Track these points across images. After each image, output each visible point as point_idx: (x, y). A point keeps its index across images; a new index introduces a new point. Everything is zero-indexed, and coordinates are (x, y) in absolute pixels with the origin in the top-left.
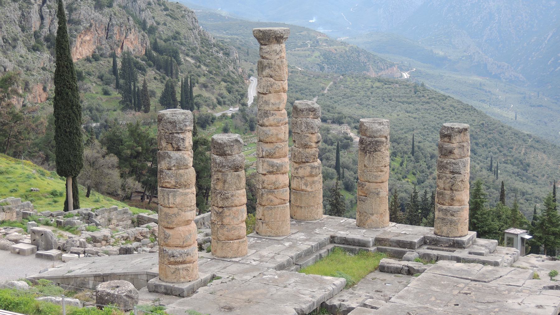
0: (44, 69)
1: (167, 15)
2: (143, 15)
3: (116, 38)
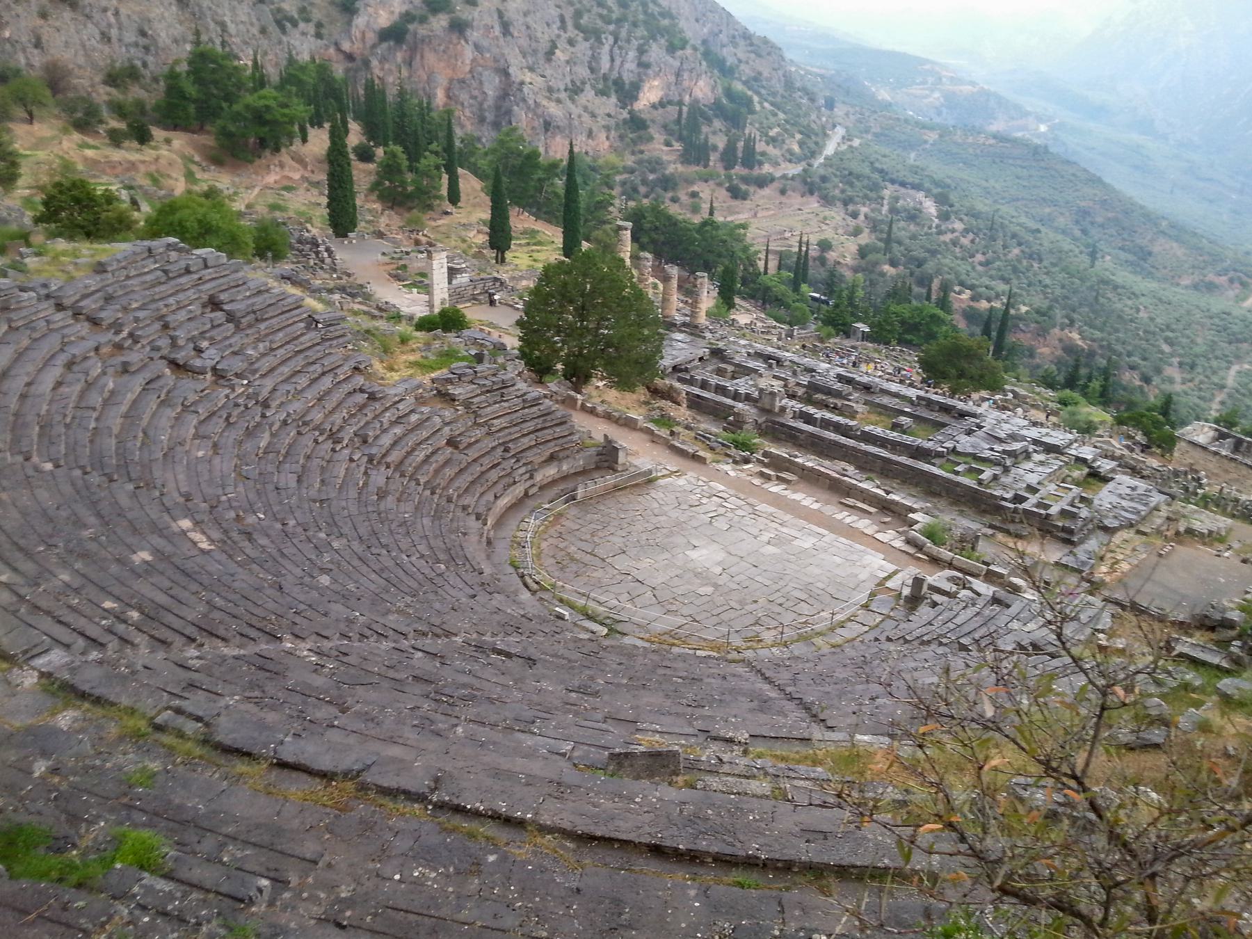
0: (609, 115)
1: (752, 52)
2: (725, 50)
3: (686, 84)
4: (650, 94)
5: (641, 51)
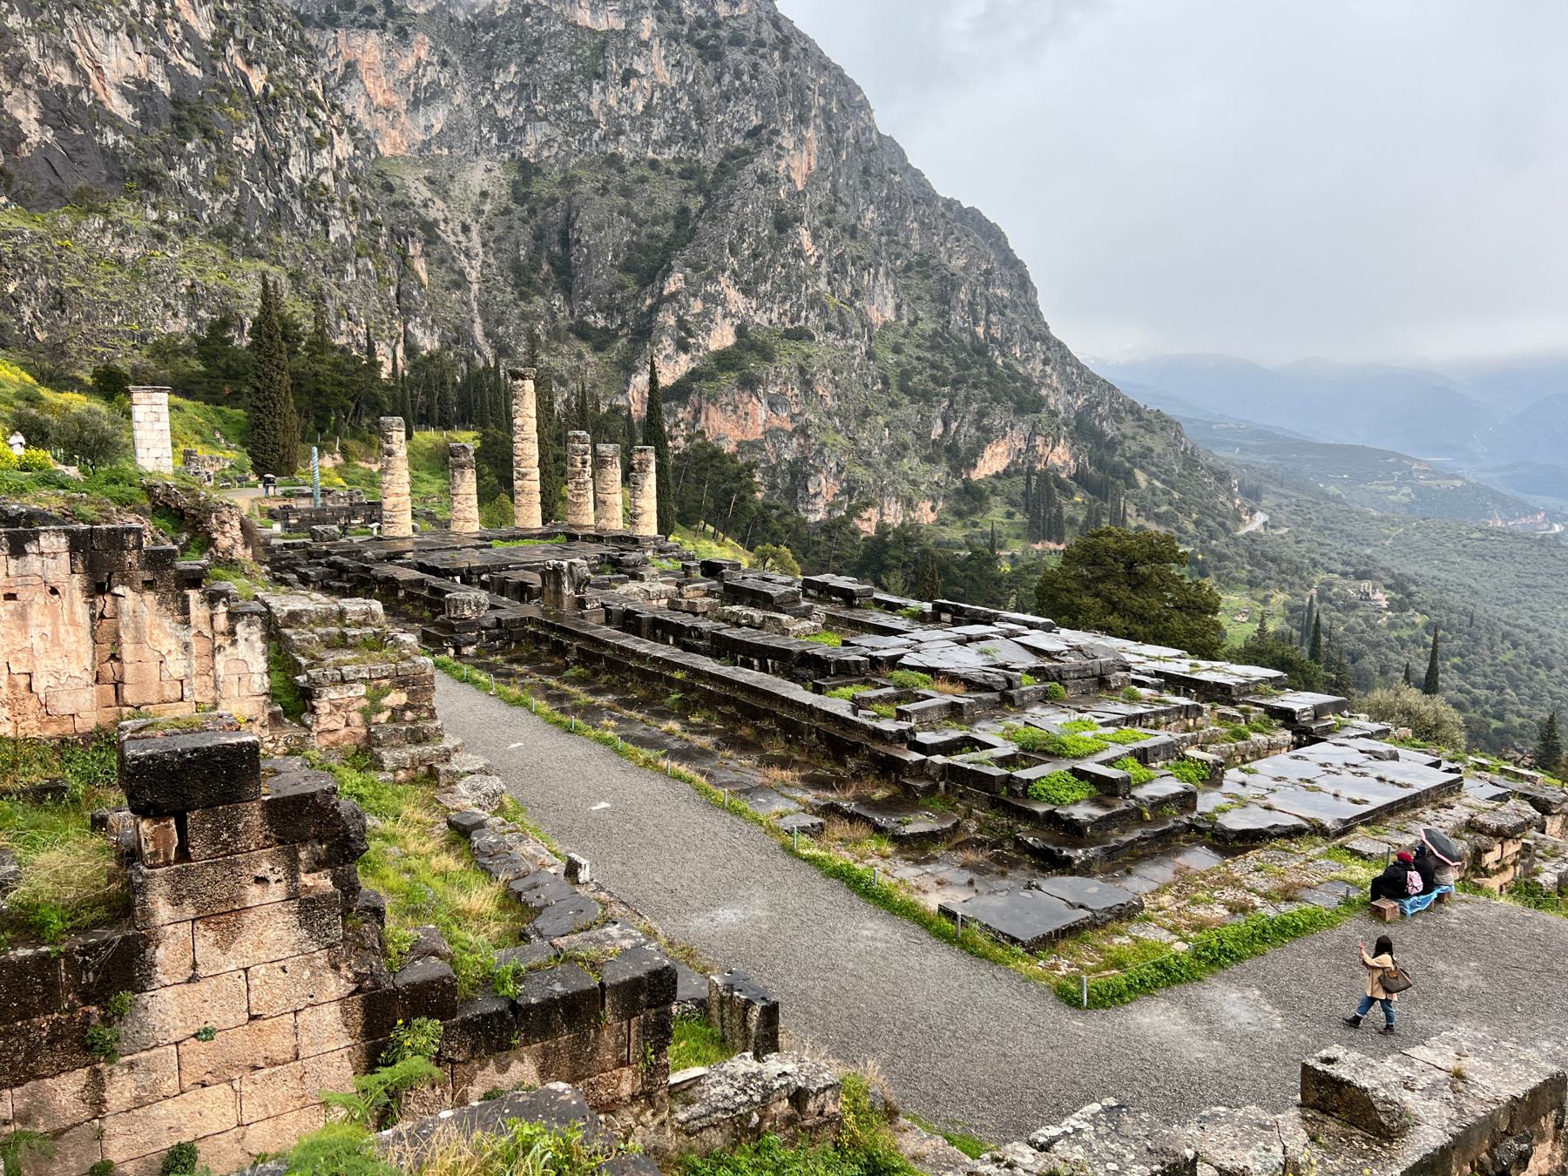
4: (993, 461)
5: (982, 414)
